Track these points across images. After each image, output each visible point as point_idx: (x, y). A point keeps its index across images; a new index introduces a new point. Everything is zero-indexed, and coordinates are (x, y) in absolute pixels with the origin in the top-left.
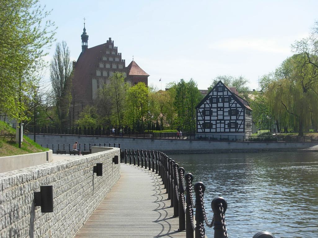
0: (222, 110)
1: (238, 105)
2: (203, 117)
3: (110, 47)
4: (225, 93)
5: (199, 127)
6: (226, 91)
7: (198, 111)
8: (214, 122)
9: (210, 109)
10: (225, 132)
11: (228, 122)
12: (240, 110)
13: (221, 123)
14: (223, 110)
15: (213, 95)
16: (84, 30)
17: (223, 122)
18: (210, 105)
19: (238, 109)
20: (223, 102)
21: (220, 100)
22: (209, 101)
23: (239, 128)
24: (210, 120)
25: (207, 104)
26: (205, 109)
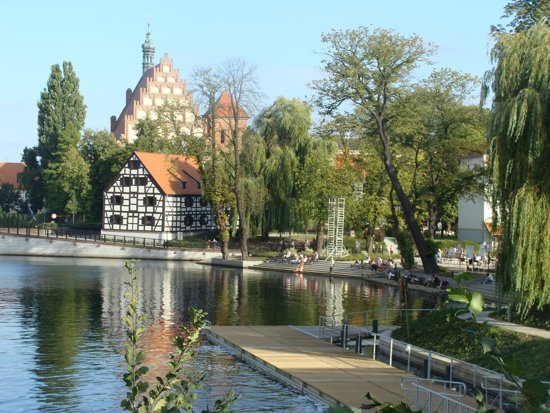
0: (135, 197)
1: (156, 191)
2: (112, 206)
3: (166, 69)
4: (141, 171)
5: (106, 221)
6: (141, 168)
7: (106, 197)
8: (124, 215)
9: (121, 195)
10: (138, 231)
11: (143, 215)
12: (158, 197)
13: (133, 216)
14: (137, 197)
15: (125, 174)
16: (148, 34)
17: (136, 214)
18: (121, 188)
19: (156, 196)
20: (137, 184)
21: (134, 180)
22: (119, 182)
23: (156, 226)
24: (121, 211)
25: (118, 186)
26: (115, 194)
